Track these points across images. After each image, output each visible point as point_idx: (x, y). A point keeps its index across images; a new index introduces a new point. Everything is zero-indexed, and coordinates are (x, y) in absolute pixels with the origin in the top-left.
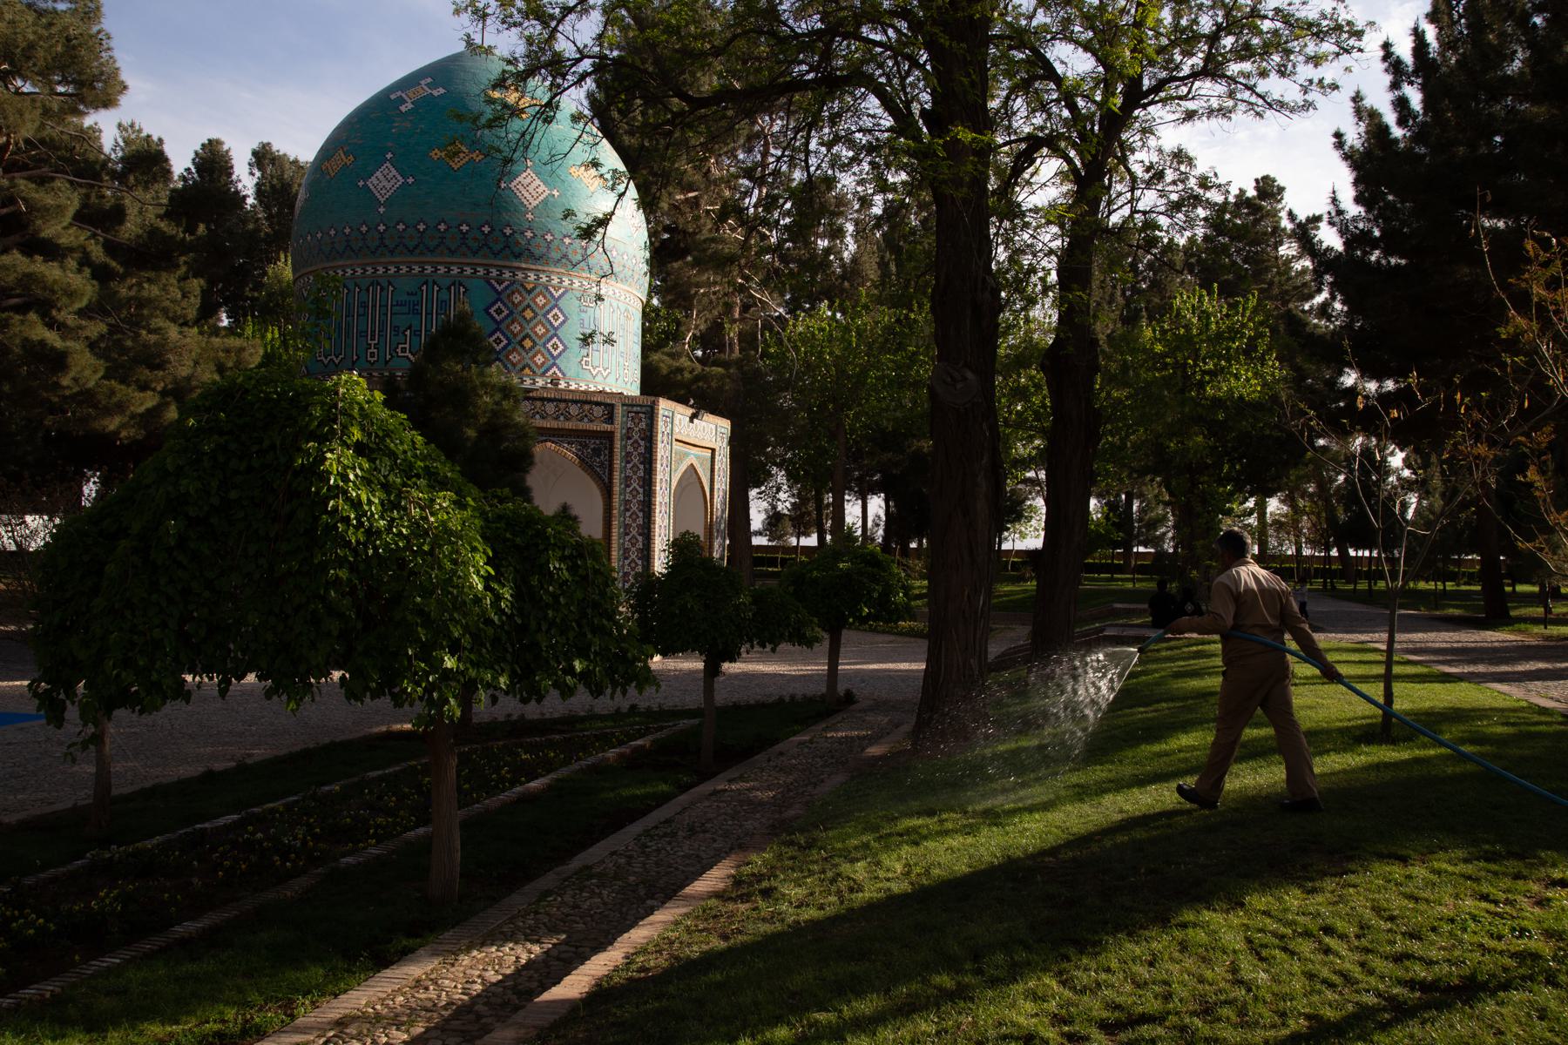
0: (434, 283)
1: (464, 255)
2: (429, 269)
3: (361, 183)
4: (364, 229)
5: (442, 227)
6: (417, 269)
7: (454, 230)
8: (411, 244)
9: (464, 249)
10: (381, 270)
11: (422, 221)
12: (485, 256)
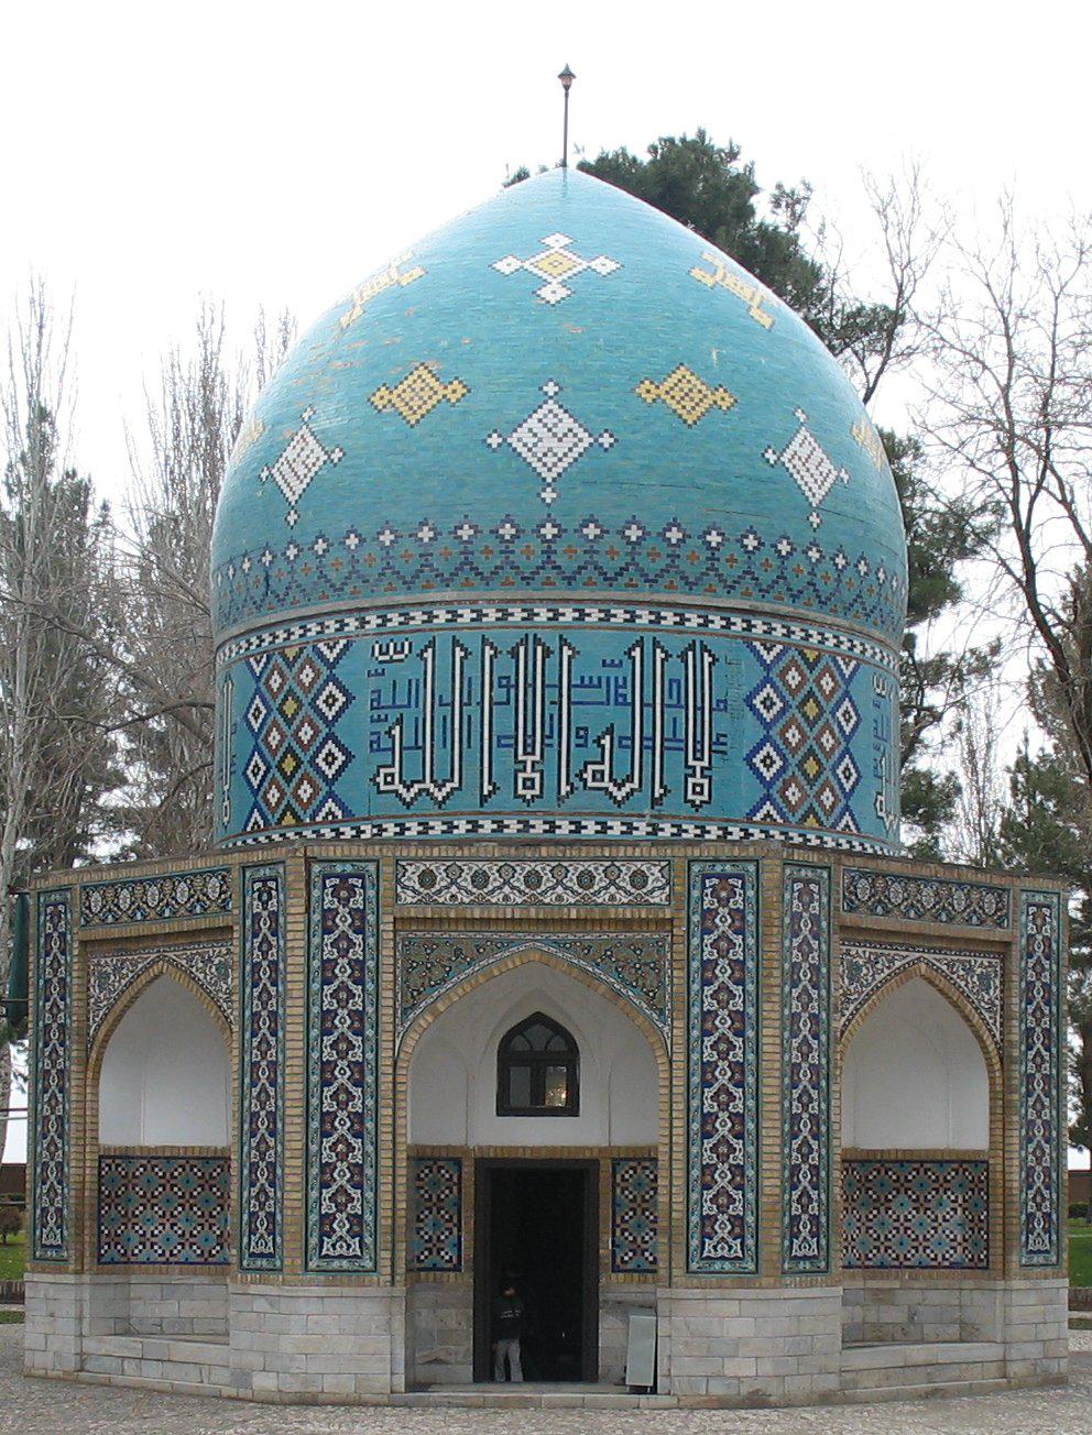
0: (656, 644)
1: (711, 590)
2: (645, 617)
3: (495, 440)
4: (507, 531)
5: (674, 535)
6: (620, 615)
7: (694, 542)
8: (611, 566)
9: (712, 578)
10: (543, 615)
11: (633, 520)
12: (746, 594)
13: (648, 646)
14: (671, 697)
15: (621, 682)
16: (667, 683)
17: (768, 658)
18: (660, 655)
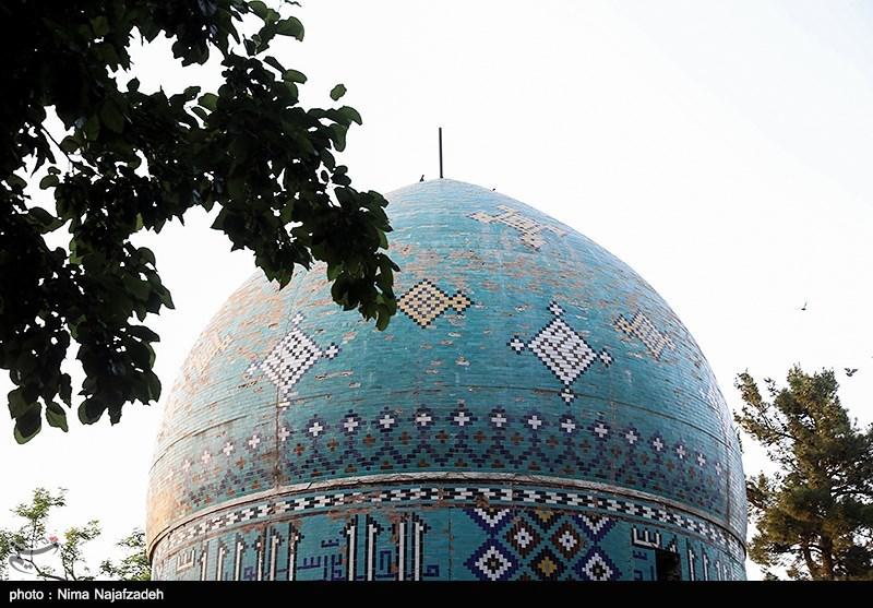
0: (370, 520)
13: (362, 522)
14: (382, 568)
15: (337, 560)
16: (378, 556)
17: (492, 523)
18: (372, 530)
